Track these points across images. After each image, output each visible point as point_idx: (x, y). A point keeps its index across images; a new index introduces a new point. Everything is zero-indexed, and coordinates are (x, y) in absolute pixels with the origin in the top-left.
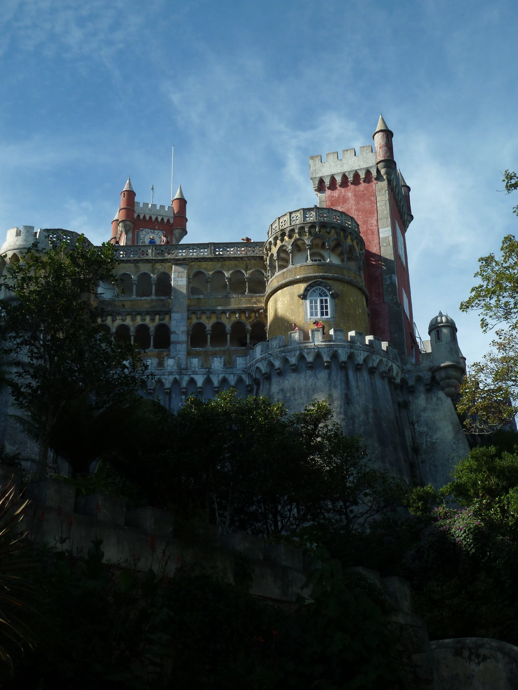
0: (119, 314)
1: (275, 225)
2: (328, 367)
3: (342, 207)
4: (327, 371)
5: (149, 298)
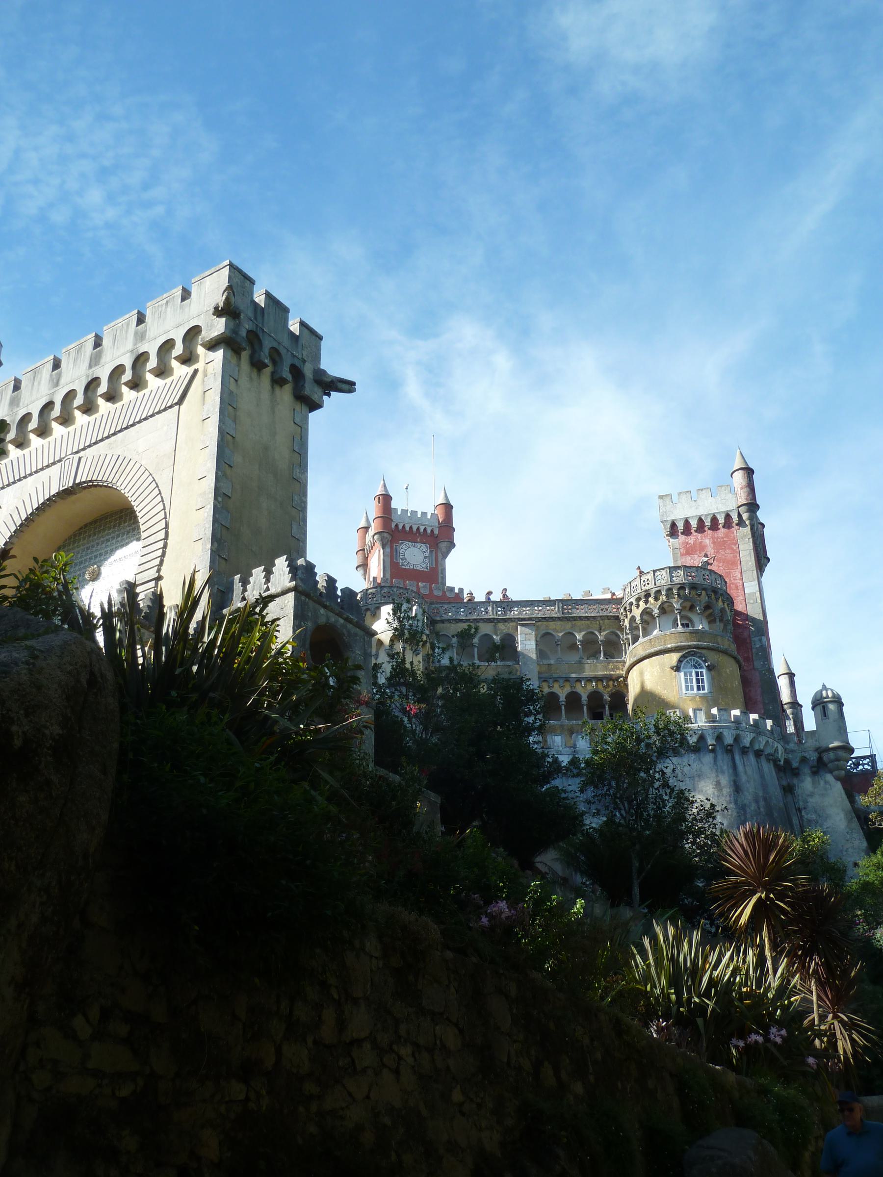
2: (713, 751)
4: (712, 755)
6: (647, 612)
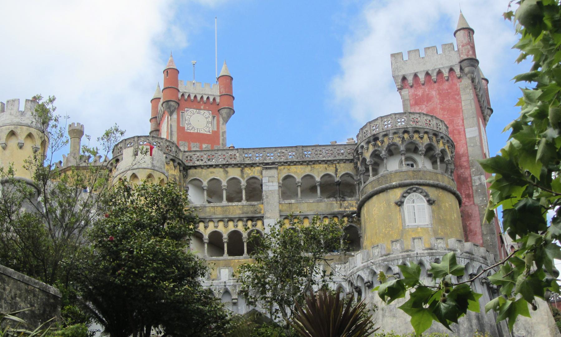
0: (211, 220)
1: (366, 129)
3: (426, 106)
5: (240, 203)
6: (375, 155)
